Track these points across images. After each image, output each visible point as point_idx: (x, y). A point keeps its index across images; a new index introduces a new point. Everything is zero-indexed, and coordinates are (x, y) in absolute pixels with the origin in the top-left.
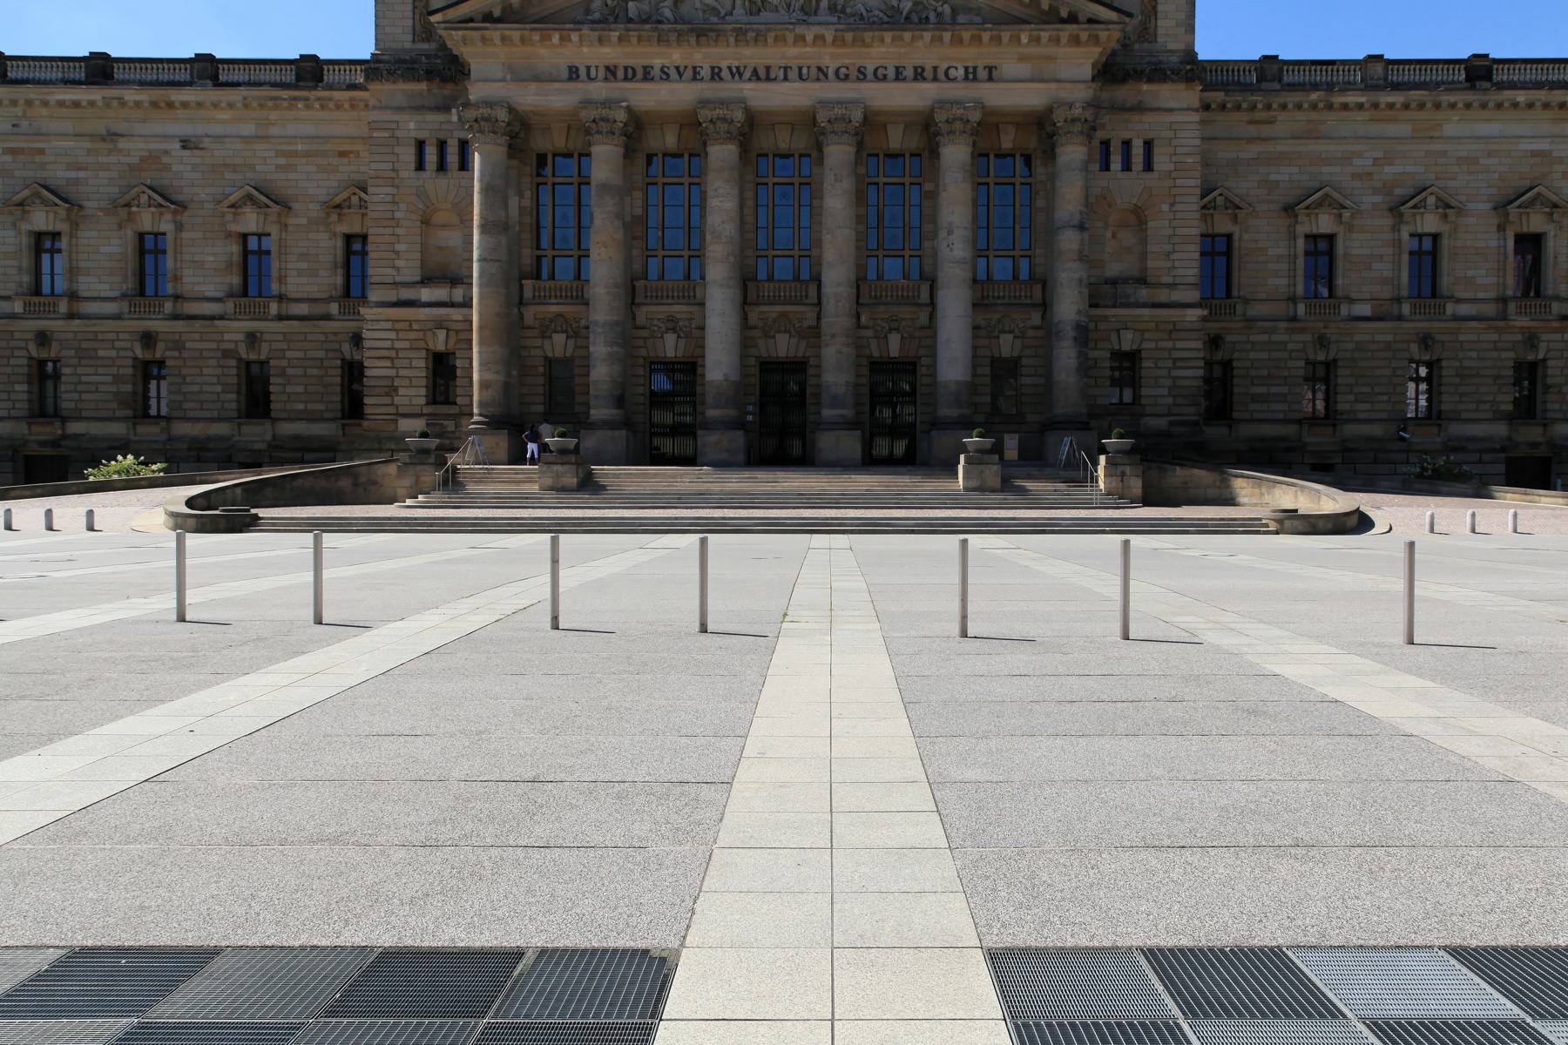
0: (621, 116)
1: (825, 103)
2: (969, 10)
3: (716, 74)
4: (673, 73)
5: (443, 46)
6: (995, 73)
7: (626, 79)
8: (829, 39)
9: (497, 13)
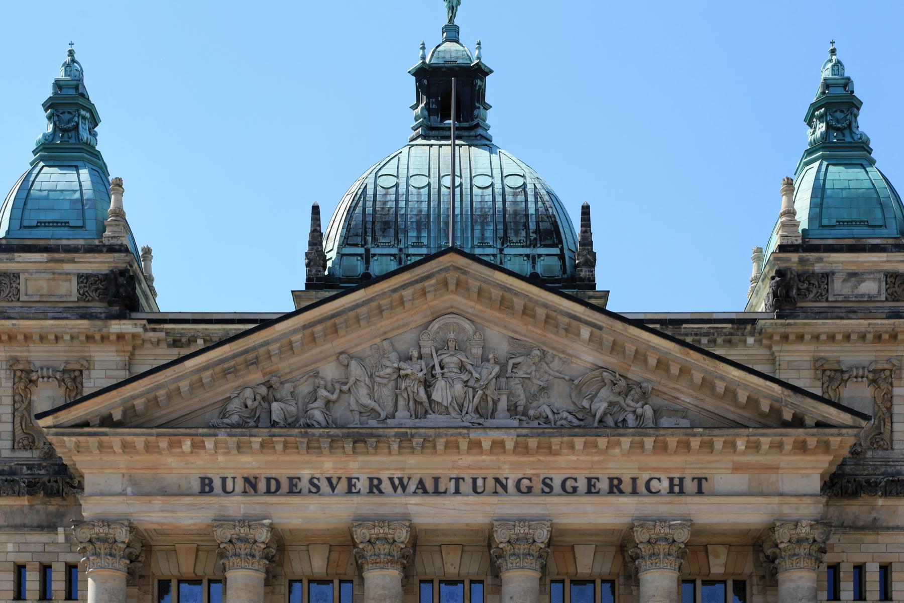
0: (263, 535)
1: (504, 521)
2: (674, 412)
3: (375, 487)
4: (325, 486)
5: (50, 453)
7: (268, 492)
8: (510, 445)
9: (117, 416)
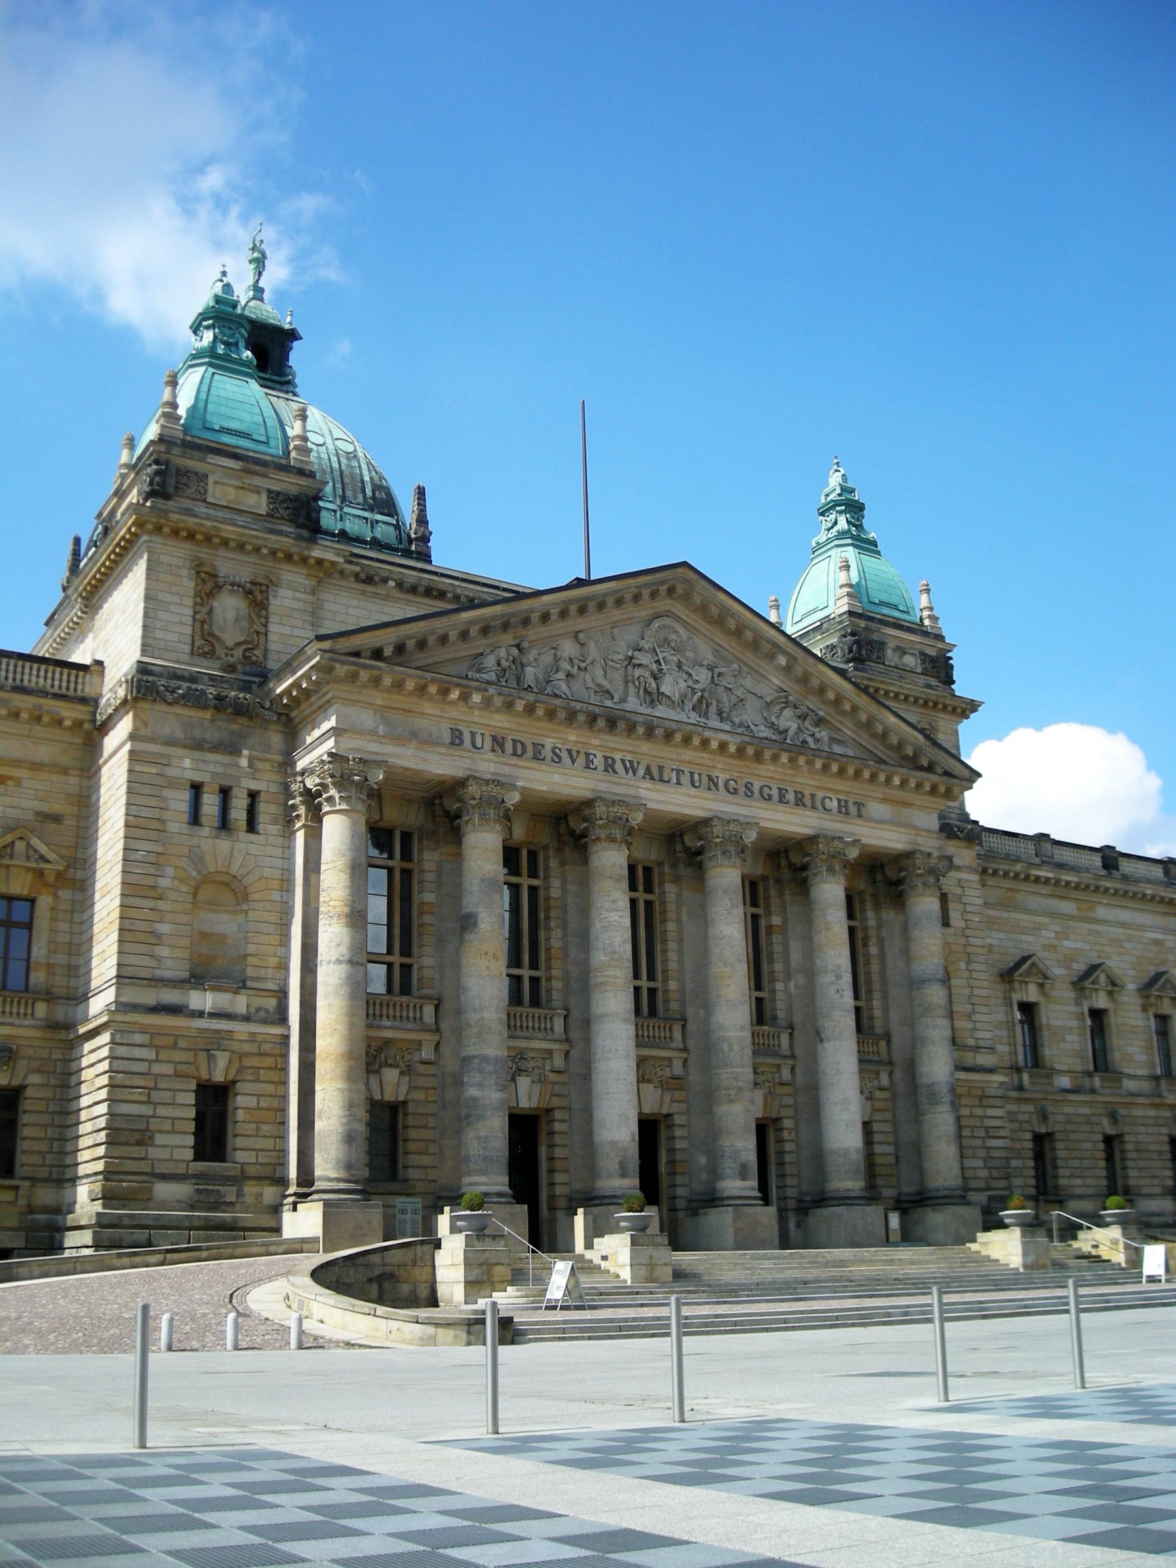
6: (863, 810)
